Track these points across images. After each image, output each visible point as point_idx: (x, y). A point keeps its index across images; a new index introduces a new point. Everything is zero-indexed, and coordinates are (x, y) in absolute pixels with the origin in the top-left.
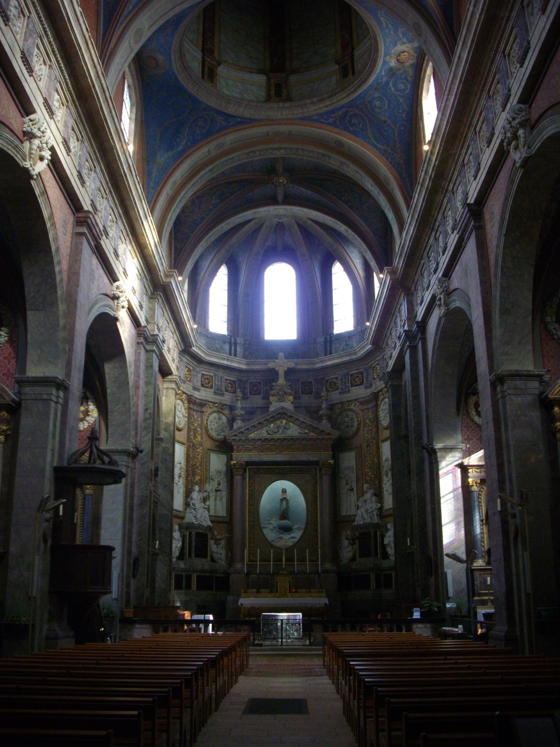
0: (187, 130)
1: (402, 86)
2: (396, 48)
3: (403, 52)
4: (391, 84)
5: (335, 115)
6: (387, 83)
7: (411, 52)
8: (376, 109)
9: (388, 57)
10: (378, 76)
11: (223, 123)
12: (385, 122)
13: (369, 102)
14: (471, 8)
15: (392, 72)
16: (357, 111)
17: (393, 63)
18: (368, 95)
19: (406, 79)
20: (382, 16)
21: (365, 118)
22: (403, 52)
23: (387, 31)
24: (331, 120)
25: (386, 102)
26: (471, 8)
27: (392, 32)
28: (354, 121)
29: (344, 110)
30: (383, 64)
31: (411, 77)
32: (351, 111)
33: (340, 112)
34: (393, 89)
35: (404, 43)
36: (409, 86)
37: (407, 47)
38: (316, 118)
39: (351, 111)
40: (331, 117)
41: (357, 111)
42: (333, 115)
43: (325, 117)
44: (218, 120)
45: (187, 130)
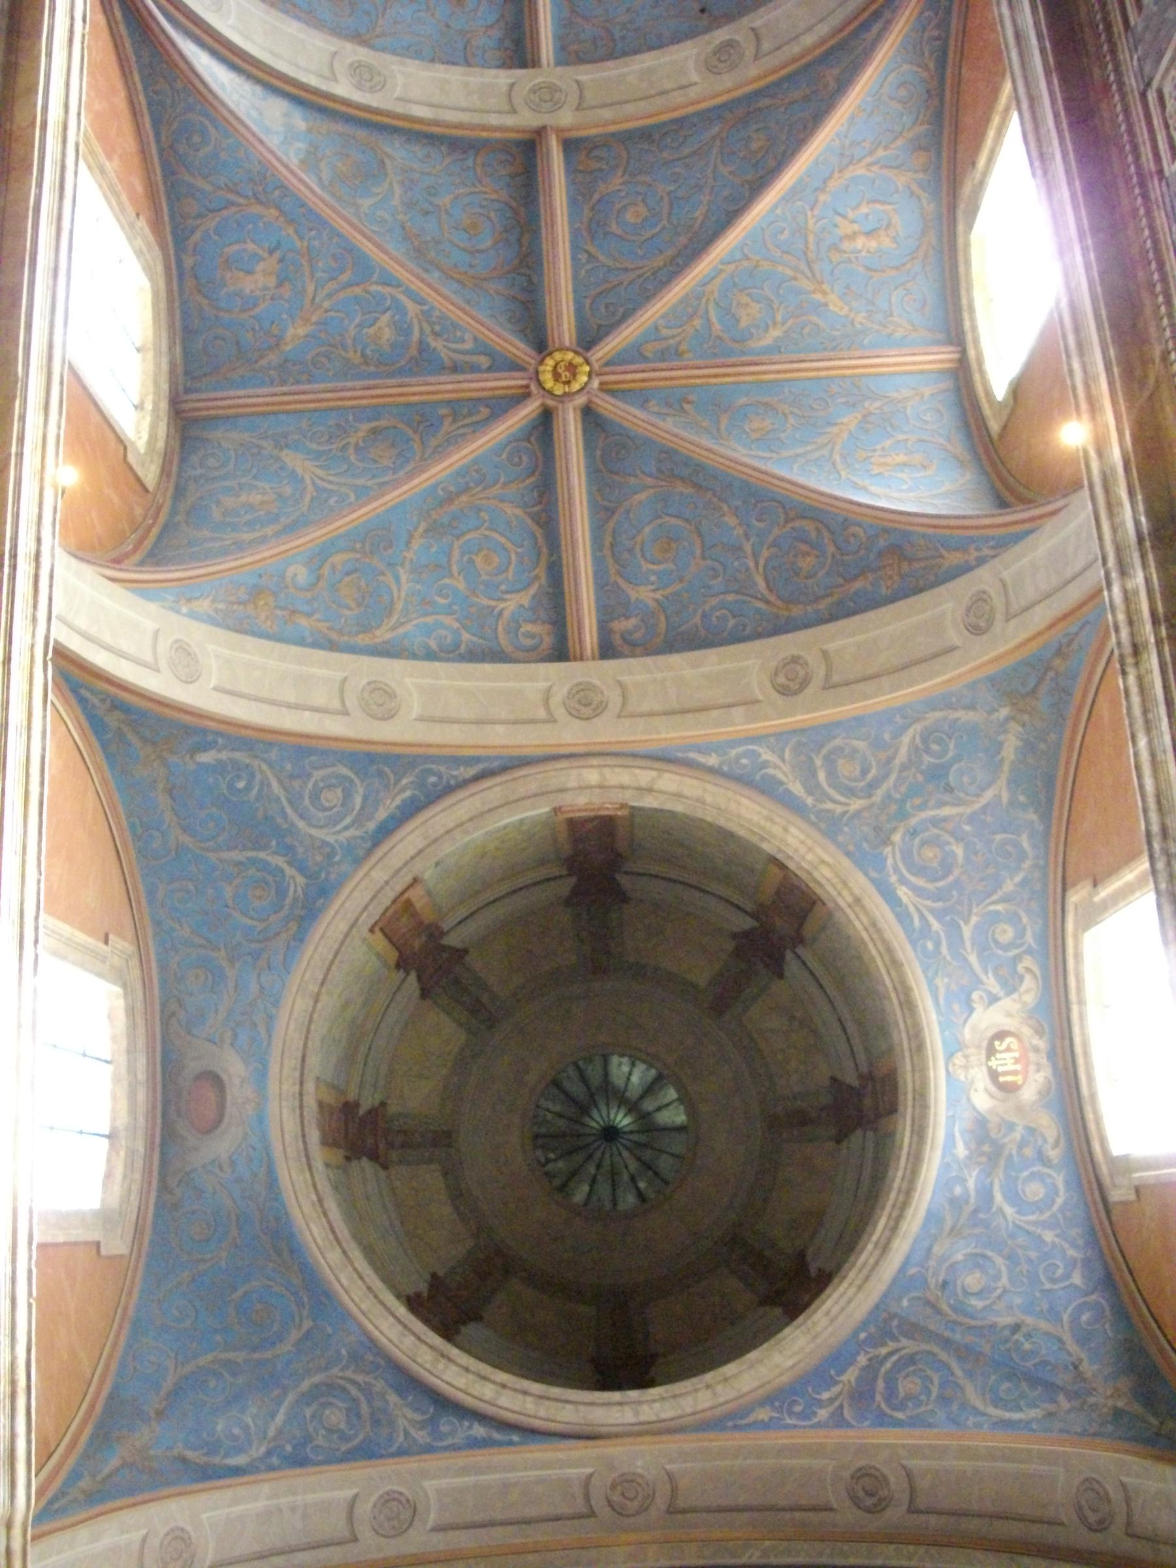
0: (280, 1418)
1: (1035, 1191)
2: (975, 1016)
3: (1001, 1035)
4: (998, 1197)
5: (836, 1389)
6: (986, 1195)
7: (1027, 1031)
8: (974, 1302)
9: (959, 1060)
10: (945, 1166)
11: (422, 1436)
12: (1016, 1328)
13: (945, 1284)
14: (1076, 365)
15: (987, 1141)
16: (908, 1346)
17: (983, 1100)
18: (932, 1263)
19: (1042, 1158)
20: (903, 881)
21: (943, 1356)
22: (1001, 1035)
23: (930, 945)
24: (823, 1414)
25: (999, 1260)
26: (1076, 365)
27: (944, 949)
28: (905, 1386)
29: (862, 1360)
30: (952, 1103)
31: (1056, 1144)
32: (892, 1353)
33: (851, 1376)
34: (1009, 1210)
35: (993, 999)
36: (1060, 1180)
37: (1009, 1015)
38: (763, 1414)
39: (892, 1353)
40: (820, 1404)
41: (908, 1346)
42: (825, 1396)
43: (798, 1409)
44: (401, 1423)
45: (280, 1418)
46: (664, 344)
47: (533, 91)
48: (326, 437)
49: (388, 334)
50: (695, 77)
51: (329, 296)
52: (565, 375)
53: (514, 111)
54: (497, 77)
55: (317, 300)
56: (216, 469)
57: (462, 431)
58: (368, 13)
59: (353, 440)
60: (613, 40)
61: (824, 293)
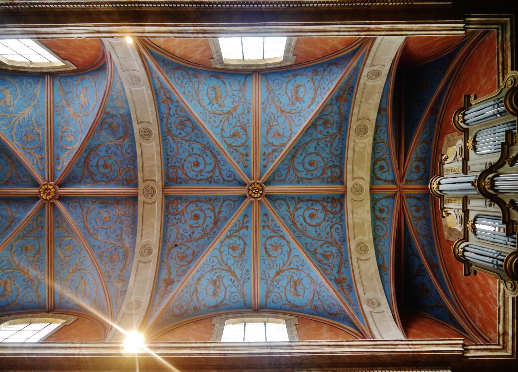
46: (61, 223)
47: (152, 188)
48: (37, 120)
49: (69, 139)
50: (144, 240)
51: (79, 122)
52: (46, 192)
53: (144, 181)
54: (158, 176)
55: (79, 118)
56: (26, 87)
57: (35, 161)
58: (180, 134)
59: (36, 128)
60: (175, 215)
61: (72, 273)
